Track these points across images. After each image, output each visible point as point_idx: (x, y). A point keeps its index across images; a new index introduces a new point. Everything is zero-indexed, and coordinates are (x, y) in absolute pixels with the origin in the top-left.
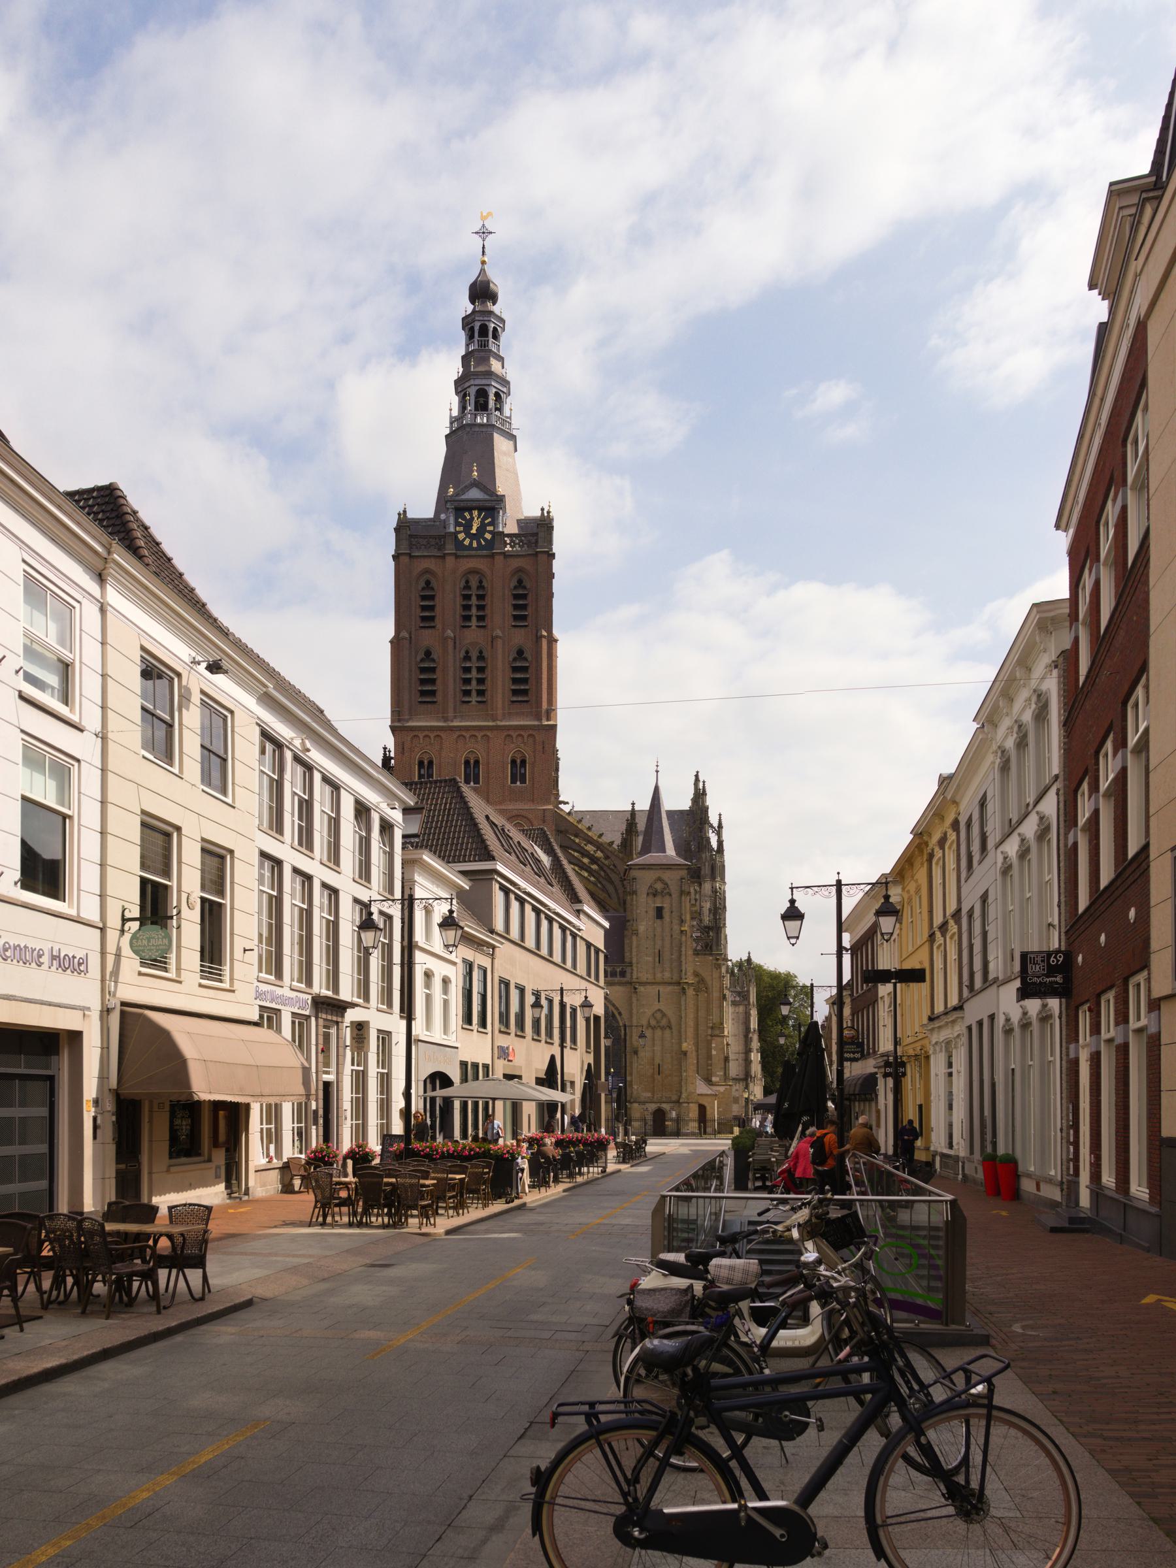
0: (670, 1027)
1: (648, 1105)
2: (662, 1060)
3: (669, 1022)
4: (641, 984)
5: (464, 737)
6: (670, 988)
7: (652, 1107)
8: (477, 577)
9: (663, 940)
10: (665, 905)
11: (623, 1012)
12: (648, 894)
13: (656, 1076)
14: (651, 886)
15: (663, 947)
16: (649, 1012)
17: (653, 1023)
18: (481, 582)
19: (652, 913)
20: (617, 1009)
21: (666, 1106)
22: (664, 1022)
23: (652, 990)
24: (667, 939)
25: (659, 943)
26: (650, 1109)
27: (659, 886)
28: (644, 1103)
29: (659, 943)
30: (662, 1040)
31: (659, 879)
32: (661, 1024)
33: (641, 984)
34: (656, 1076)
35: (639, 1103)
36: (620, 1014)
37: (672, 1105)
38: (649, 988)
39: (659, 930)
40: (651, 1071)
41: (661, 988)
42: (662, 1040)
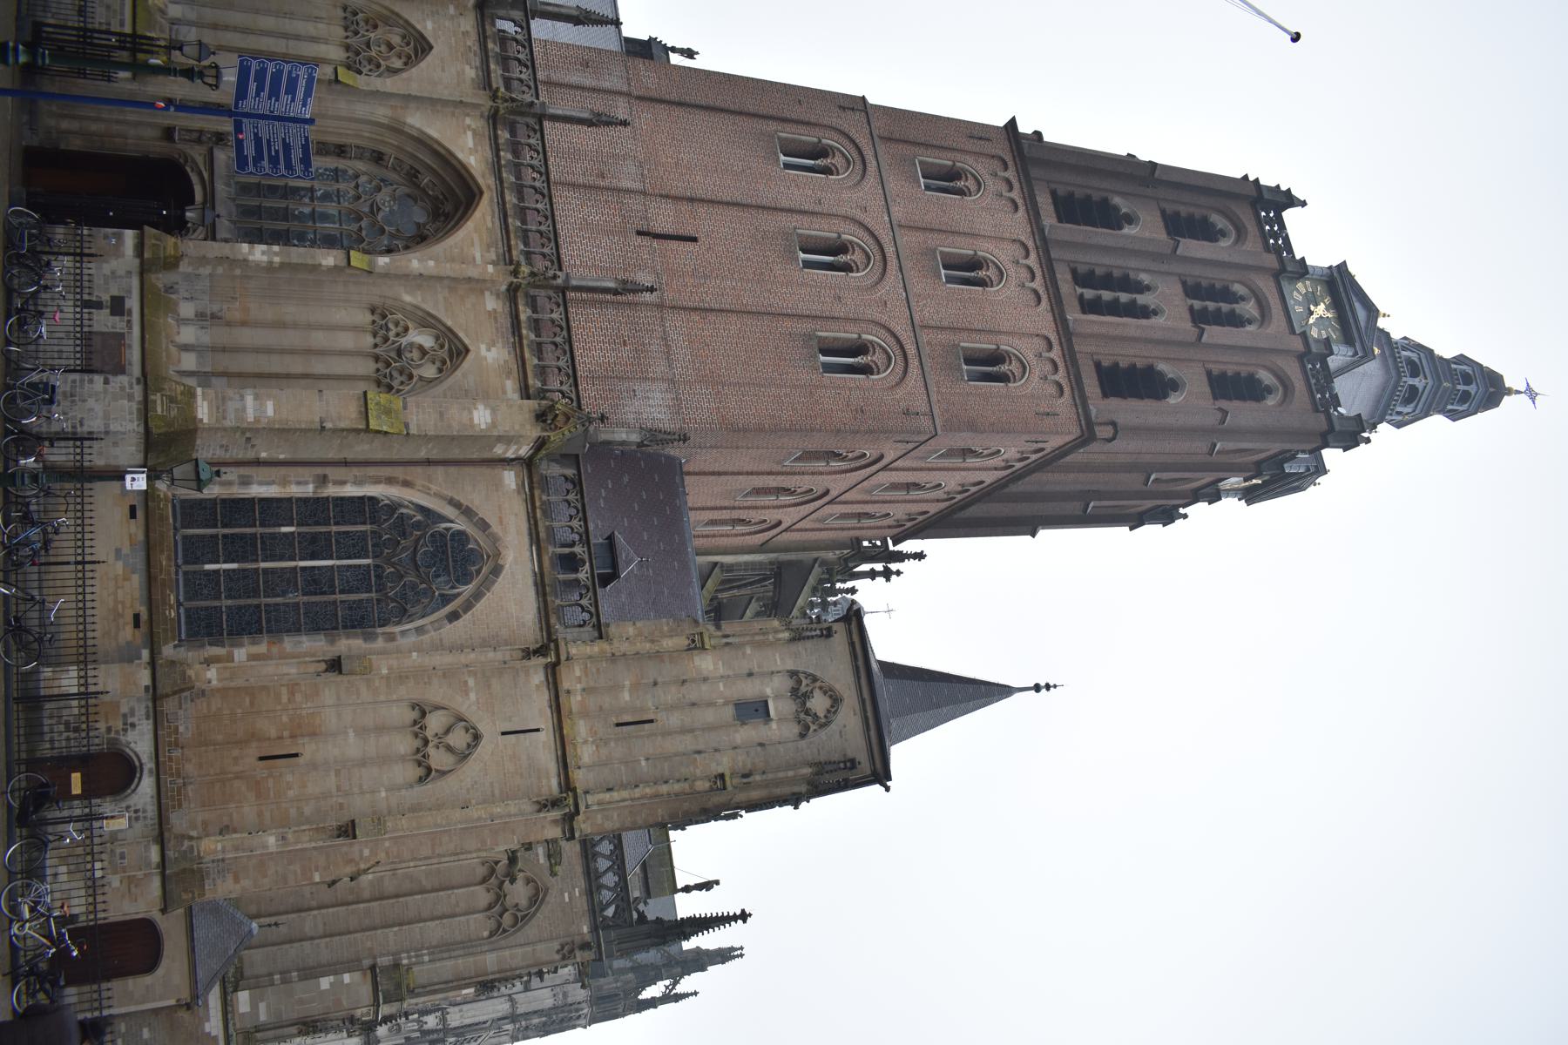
0: (427, 773)
1: (146, 727)
2: (314, 766)
3: (443, 773)
4: (552, 671)
5: (1027, 256)
6: (549, 762)
7: (140, 743)
8: (1255, 313)
9: (684, 731)
10: (774, 725)
11: (459, 623)
12: (793, 674)
13: (253, 751)
14: (815, 679)
15: (667, 733)
16: (469, 704)
17: (435, 723)
18: (1250, 322)
19: (750, 690)
20: (468, 606)
21: (146, 786)
22: (438, 758)
23: (536, 710)
24: (686, 743)
25: (674, 720)
26: (131, 736)
27: (818, 703)
28: (156, 717)
29: (674, 720)
30: (385, 760)
31: (836, 701)
32: (431, 750)
33: (552, 671)
34: (253, 751)
35: (155, 694)
36: (454, 616)
37: (151, 810)
38: (542, 699)
39: (709, 716)
40: (273, 733)
41: (546, 737)
42: (385, 760)
